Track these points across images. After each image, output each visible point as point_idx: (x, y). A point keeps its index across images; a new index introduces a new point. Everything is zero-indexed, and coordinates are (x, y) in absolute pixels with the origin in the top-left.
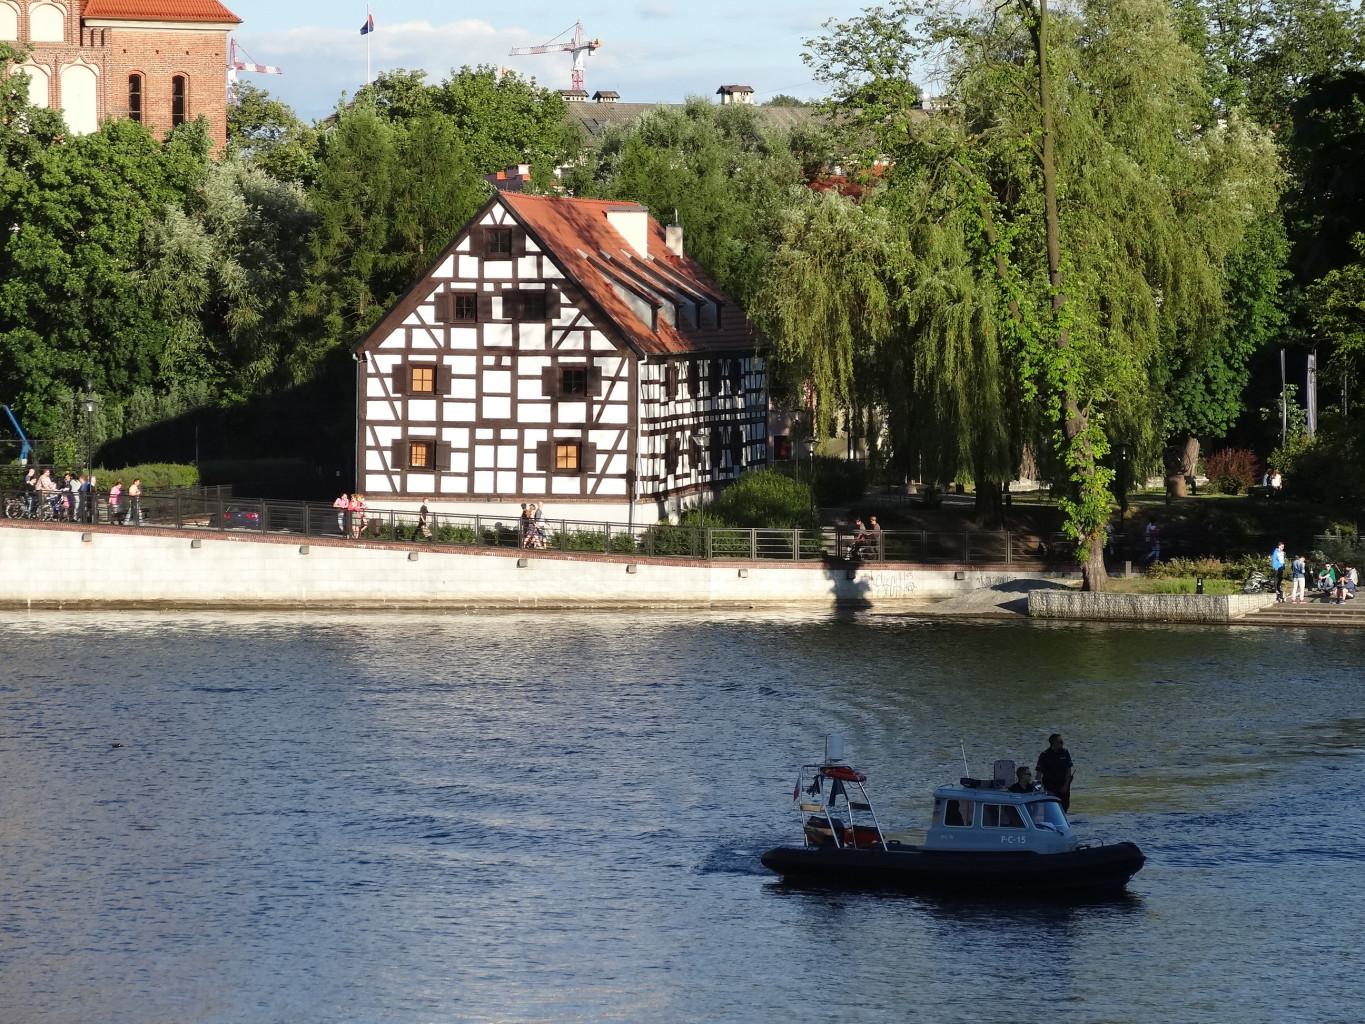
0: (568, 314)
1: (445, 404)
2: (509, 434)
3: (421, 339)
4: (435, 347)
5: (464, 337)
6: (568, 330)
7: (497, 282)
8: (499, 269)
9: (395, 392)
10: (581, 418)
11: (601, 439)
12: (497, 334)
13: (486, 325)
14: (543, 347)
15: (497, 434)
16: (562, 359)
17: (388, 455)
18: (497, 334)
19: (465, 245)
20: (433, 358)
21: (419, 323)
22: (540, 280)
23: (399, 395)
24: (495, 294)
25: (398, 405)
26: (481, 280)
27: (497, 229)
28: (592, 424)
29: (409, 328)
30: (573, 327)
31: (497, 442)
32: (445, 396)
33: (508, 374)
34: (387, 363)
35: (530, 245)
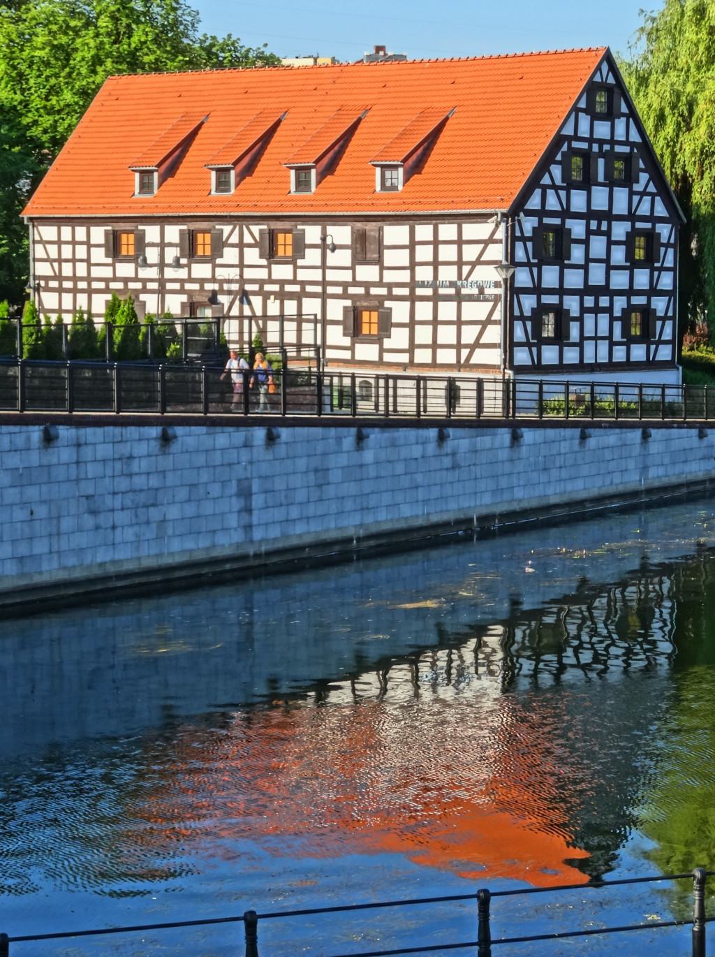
0: (644, 177)
1: (566, 271)
2: (604, 301)
3: (553, 203)
5: (578, 201)
6: (643, 193)
7: (601, 142)
8: (602, 129)
9: (533, 258)
10: (647, 287)
11: (659, 304)
12: (600, 198)
13: (594, 188)
14: (626, 213)
15: (597, 302)
16: (639, 225)
18: (600, 198)
19: (582, 105)
20: (557, 221)
21: (550, 183)
22: (626, 143)
23: (536, 261)
24: (602, 154)
25: (535, 270)
26: (591, 140)
27: (603, 86)
29: (544, 188)
30: (643, 193)
31: (596, 310)
32: (566, 262)
33: (604, 238)
34: (529, 224)
35: (624, 109)
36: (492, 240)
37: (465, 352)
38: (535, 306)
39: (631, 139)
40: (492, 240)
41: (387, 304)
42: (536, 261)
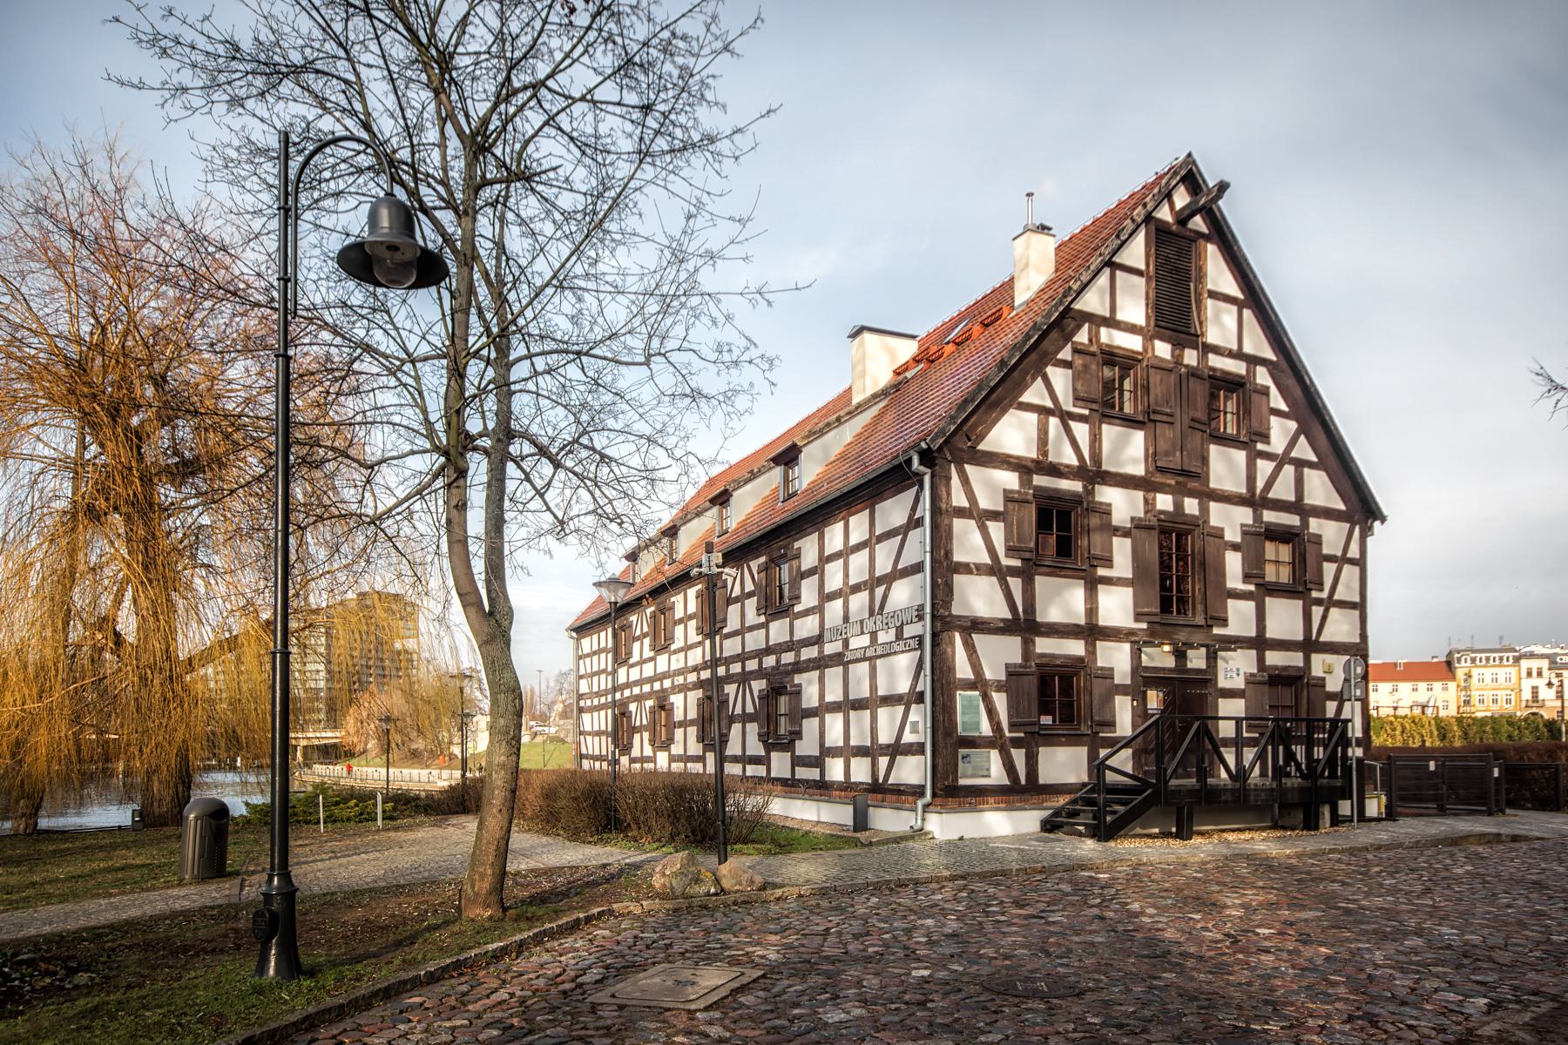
4: (1074, 462)
17: (1000, 700)
20: (1075, 486)
22: (1238, 355)
23: (1017, 563)
25: (1015, 584)
28: (1310, 645)
32: (1101, 572)
36: (914, 523)
37: (883, 762)
38: (1017, 659)
39: (1248, 349)
40: (914, 523)
41: (798, 679)
42: (1017, 563)
